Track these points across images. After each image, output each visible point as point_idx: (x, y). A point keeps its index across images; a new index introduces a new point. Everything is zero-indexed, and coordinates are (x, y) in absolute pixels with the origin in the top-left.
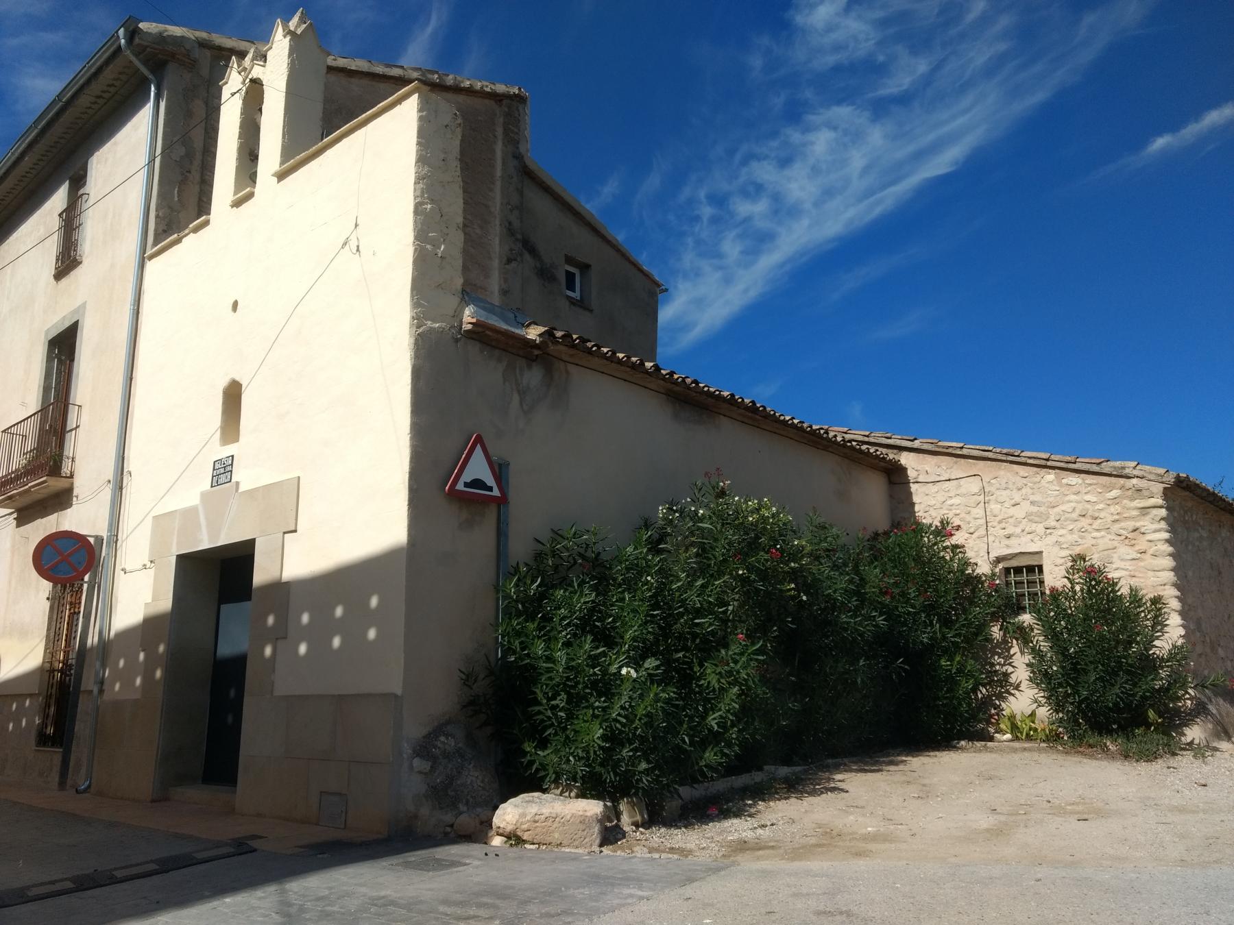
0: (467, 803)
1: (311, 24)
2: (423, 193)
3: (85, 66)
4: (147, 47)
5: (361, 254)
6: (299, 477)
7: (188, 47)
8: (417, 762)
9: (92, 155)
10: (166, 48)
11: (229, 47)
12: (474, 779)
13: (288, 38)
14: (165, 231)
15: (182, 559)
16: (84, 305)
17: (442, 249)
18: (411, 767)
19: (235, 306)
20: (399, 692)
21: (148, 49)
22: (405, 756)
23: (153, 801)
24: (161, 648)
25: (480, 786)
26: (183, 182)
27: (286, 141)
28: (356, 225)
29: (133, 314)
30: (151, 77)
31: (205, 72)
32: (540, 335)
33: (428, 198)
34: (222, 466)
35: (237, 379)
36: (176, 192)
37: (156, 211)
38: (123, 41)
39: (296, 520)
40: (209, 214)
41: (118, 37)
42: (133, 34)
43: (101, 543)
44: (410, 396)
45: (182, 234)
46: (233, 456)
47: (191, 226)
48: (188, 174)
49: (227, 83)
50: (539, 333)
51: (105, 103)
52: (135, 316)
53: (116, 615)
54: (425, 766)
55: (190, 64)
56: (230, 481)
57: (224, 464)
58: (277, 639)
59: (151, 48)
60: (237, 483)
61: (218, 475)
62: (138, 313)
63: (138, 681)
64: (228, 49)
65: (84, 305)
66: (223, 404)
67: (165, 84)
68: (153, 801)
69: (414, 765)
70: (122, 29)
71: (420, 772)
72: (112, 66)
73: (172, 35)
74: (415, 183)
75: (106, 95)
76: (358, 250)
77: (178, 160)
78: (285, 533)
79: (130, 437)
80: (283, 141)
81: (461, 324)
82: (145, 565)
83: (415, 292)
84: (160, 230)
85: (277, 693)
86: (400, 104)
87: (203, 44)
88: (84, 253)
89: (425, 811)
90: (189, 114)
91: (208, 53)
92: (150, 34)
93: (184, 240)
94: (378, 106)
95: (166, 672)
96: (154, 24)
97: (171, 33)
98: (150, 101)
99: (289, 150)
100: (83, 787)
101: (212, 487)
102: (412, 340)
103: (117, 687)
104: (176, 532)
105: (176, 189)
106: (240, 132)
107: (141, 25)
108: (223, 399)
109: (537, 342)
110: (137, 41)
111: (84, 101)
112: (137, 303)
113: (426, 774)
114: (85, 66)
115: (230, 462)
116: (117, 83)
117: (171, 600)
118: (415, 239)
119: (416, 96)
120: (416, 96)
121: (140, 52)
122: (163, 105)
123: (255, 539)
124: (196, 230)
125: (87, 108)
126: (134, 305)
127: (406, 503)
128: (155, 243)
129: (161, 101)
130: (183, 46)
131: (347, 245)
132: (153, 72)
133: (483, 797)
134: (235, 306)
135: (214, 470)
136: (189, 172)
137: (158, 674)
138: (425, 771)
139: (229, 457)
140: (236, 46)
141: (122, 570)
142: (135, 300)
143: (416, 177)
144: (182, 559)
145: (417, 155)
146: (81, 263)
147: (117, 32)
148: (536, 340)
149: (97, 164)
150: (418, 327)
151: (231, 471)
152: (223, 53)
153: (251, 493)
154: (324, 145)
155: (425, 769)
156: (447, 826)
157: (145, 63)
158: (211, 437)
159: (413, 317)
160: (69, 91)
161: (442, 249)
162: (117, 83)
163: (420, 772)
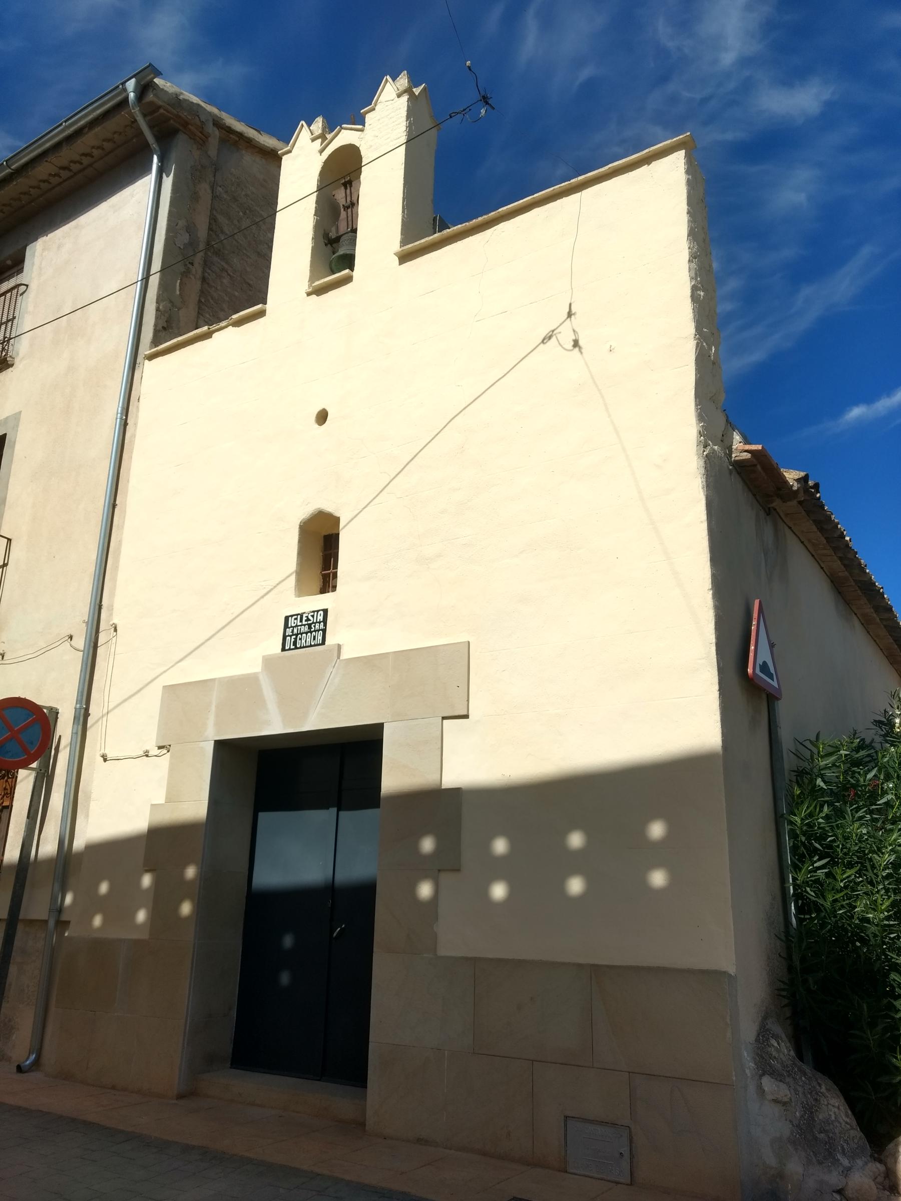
0: (844, 1153)
1: (424, 89)
2: (696, 274)
3: (62, 124)
4: (159, 107)
5: (583, 351)
6: (469, 642)
7: (203, 118)
8: (768, 1083)
9: (36, 239)
10: (180, 114)
11: (238, 130)
12: (836, 1110)
13: (405, 98)
14: (164, 328)
15: (223, 748)
16: (17, 417)
17: (713, 352)
18: (761, 1091)
19: (322, 417)
20: (732, 970)
21: (162, 111)
22: (747, 1071)
23: (180, 1097)
24: (191, 872)
25: (847, 1123)
26: (186, 274)
27: (405, 216)
28: (570, 314)
29: (120, 424)
30: (154, 146)
31: (213, 152)
32: (798, 480)
33: (701, 282)
34: (304, 623)
35: (329, 508)
36: (178, 284)
37: (157, 303)
38: (132, 95)
39: (468, 701)
40: (266, 304)
41: (125, 90)
42: (144, 88)
43: (55, 717)
44: (707, 538)
45: (214, 327)
46: (325, 612)
47: (235, 317)
48: (190, 266)
49: (290, 152)
50: (796, 477)
51: (69, 178)
52: (122, 427)
53: (87, 816)
54: (783, 1091)
55: (201, 141)
56: (323, 643)
57: (308, 620)
58: (439, 871)
59: (164, 110)
60: (339, 647)
61: (297, 635)
62: (125, 424)
63: (141, 916)
64: (237, 132)
65: (17, 417)
66: (299, 542)
67: (174, 155)
68: (180, 1097)
69: (766, 1089)
70: (133, 80)
71: (776, 1101)
72: (99, 128)
73: (188, 100)
74: (689, 261)
75: (75, 167)
76: (576, 344)
77: (182, 248)
78: (444, 718)
79: (114, 580)
80: (403, 216)
81: (730, 448)
82: (147, 751)
83: (698, 400)
84: (160, 327)
85: (442, 952)
86: (649, 164)
87: (218, 124)
88: (18, 354)
89: (795, 1167)
90: (195, 197)
91: (217, 132)
92: (166, 92)
93: (215, 335)
94: (610, 165)
95: (198, 909)
96: (169, 84)
97: (186, 98)
98: (151, 173)
99: (410, 231)
100: (28, 1062)
101: (283, 649)
102: (702, 463)
103: (97, 921)
104: (213, 708)
105: (179, 281)
106: (316, 207)
107: (156, 80)
108: (299, 535)
109: (795, 488)
110: (150, 97)
111: (43, 170)
112: (125, 411)
113: (784, 1104)
114: (62, 124)
115: (321, 618)
116: (96, 152)
117: (207, 801)
118: (696, 331)
119: (682, 153)
120: (682, 153)
121: (150, 111)
122: (168, 183)
123: (383, 724)
124: (239, 323)
125: (41, 181)
126: (122, 414)
127: (717, 687)
128: (156, 341)
129: (164, 175)
130: (198, 116)
131: (554, 337)
132: (159, 138)
133: (856, 1141)
134: (322, 417)
135: (286, 626)
136: (192, 264)
137: (186, 908)
138: (786, 1099)
139: (318, 611)
140: (245, 131)
141: (103, 756)
142: (123, 408)
143: (690, 253)
144: (223, 748)
145: (688, 227)
146: (12, 365)
147: (123, 83)
148: (793, 485)
149: (44, 250)
150: (705, 447)
151: (324, 631)
152: (231, 136)
153: (370, 663)
154: (498, 215)
155: (786, 1096)
156: (834, 1192)
157: (151, 127)
158: (278, 584)
159: (700, 432)
160: (24, 157)
161: (713, 352)
162: (96, 152)
163: (776, 1101)
